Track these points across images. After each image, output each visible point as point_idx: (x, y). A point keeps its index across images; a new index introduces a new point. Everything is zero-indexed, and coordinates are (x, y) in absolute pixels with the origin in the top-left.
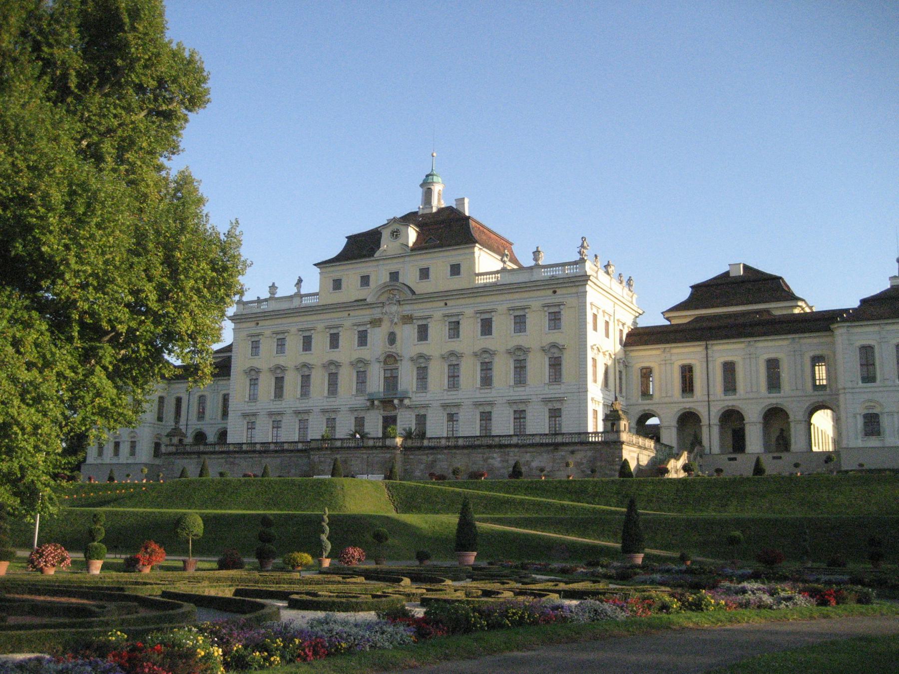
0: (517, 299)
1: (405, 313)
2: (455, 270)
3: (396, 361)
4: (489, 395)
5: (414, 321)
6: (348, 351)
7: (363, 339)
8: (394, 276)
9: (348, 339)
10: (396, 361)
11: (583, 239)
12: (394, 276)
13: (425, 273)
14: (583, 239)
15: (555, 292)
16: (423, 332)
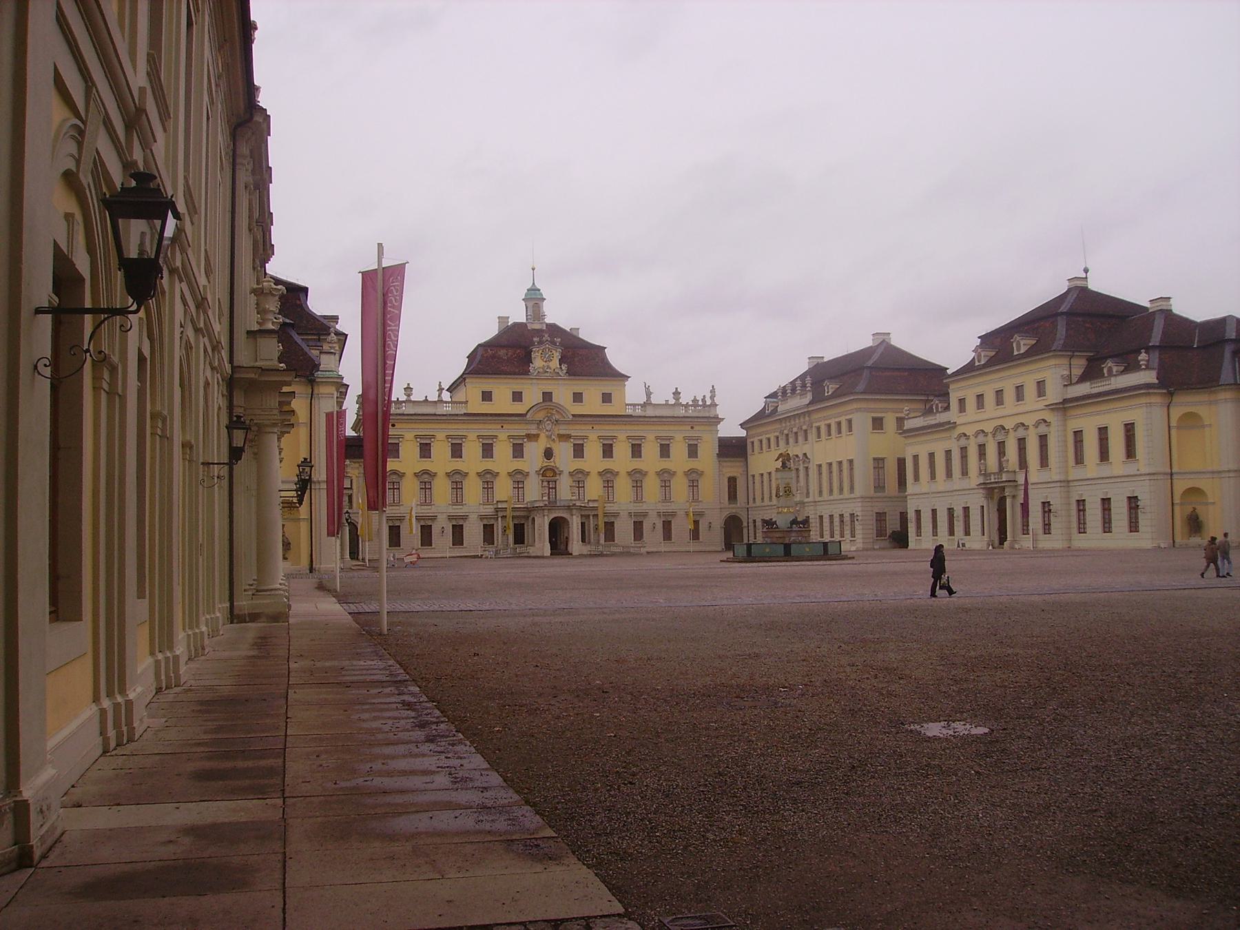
0: (664, 431)
1: (562, 432)
2: (607, 398)
3: (555, 474)
4: (611, 508)
6: (503, 460)
7: (518, 451)
8: (547, 396)
9: (503, 450)
10: (555, 474)
11: (713, 386)
12: (547, 396)
13: (578, 397)
14: (713, 386)
15: (692, 428)
16: (579, 451)
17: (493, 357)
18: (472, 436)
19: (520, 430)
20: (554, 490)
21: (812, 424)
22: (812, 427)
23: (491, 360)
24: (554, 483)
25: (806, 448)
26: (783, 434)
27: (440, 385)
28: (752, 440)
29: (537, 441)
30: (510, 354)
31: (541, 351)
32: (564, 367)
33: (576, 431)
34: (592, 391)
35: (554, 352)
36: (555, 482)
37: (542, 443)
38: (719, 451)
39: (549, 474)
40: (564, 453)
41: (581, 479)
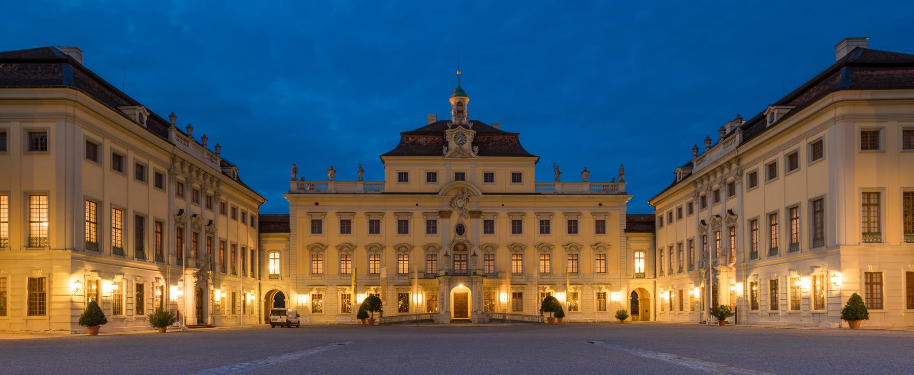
5: (482, 217)
7: (431, 227)
9: (418, 225)
16: (489, 227)
17: (413, 143)
18: (389, 214)
19: (434, 205)
20: (465, 263)
21: (742, 172)
22: (741, 175)
23: (411, 147)
24: (465, 256)
25: (732, 204)
26: (698, 196)
27: (360, 168)
28: (659, 215)
29: (449, 217)
30: (429, 142)
31: (454, 135)
32: (476, 149)
33: (488, 206)
34: (503, 168)
35: (467, 135)
36: (467, 255)
37: (455, 219)
38: (627, 227)
39: (460, 247)
40: (474, 227)
41: (491, 253)
